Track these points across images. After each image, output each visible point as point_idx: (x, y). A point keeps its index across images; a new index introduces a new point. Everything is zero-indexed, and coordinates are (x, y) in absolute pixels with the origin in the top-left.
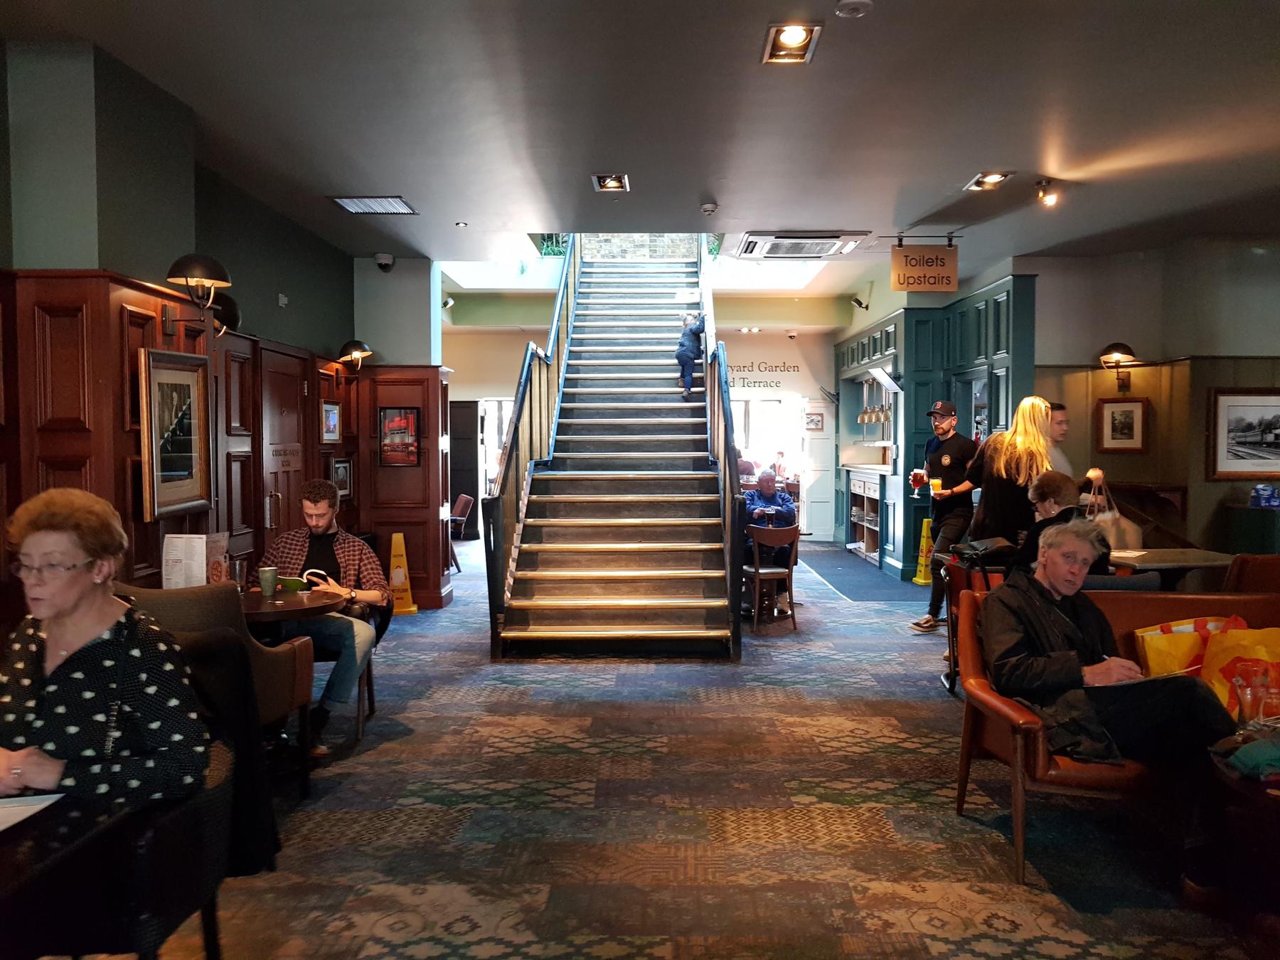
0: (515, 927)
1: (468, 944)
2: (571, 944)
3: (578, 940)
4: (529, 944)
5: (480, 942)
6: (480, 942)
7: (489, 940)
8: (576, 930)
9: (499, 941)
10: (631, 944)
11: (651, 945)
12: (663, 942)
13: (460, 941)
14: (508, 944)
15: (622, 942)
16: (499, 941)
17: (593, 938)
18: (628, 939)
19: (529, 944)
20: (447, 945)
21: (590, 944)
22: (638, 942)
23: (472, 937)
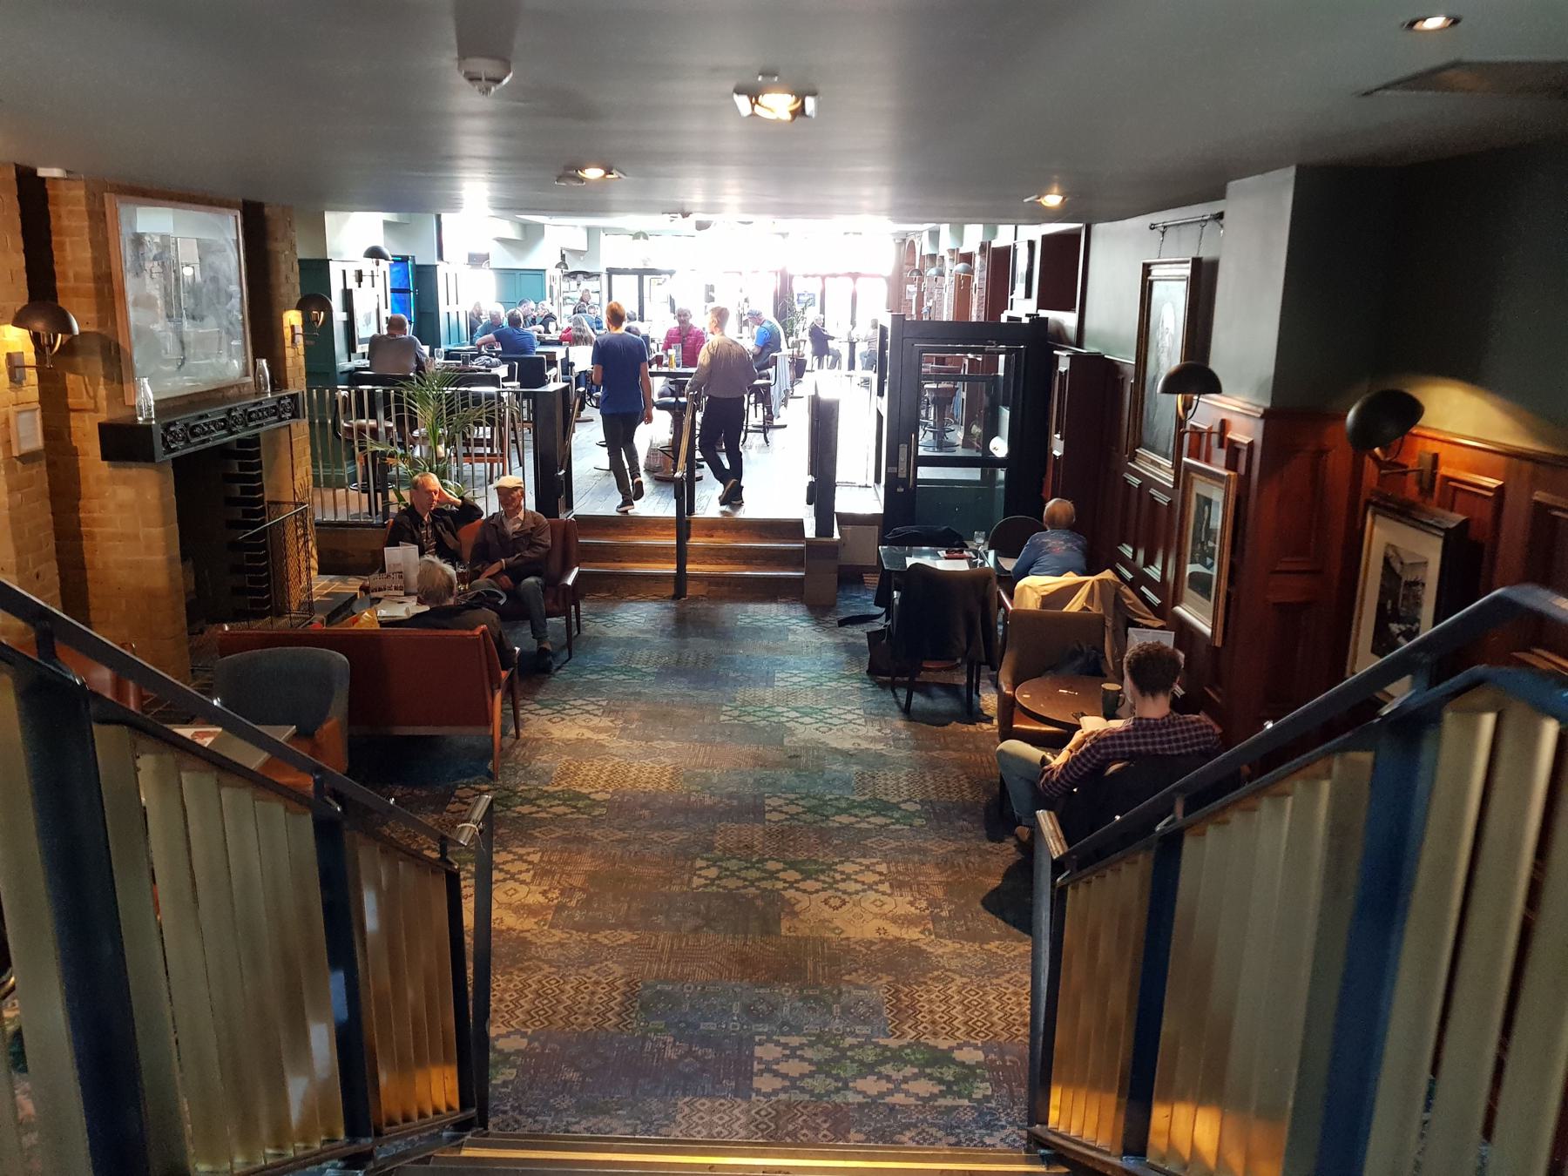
0: (799, 902)
1: (824, 889)
2: (758, 888)
3: (752, 890)
4: (785, 889)
5: (817, 891)
6: (817, 891)
7: (811, 893)
8: (756, 897)
9: (805, 891)
10: (718, 886)
11: (706, 886)
12: (698, 888)
13: (830, 892)
14: (797, 889)
15: (725, 888)
16: (805, 891)
17: (742, 891)
18: (721, 890)
19: (785, 889)
20: (837, 890)
21: (745, 887)
22: (714, 888)
23: (823, 895)
